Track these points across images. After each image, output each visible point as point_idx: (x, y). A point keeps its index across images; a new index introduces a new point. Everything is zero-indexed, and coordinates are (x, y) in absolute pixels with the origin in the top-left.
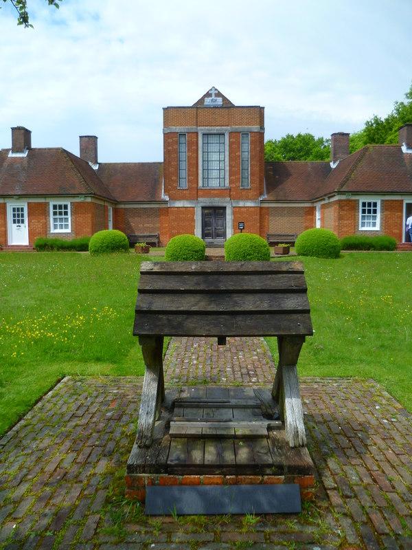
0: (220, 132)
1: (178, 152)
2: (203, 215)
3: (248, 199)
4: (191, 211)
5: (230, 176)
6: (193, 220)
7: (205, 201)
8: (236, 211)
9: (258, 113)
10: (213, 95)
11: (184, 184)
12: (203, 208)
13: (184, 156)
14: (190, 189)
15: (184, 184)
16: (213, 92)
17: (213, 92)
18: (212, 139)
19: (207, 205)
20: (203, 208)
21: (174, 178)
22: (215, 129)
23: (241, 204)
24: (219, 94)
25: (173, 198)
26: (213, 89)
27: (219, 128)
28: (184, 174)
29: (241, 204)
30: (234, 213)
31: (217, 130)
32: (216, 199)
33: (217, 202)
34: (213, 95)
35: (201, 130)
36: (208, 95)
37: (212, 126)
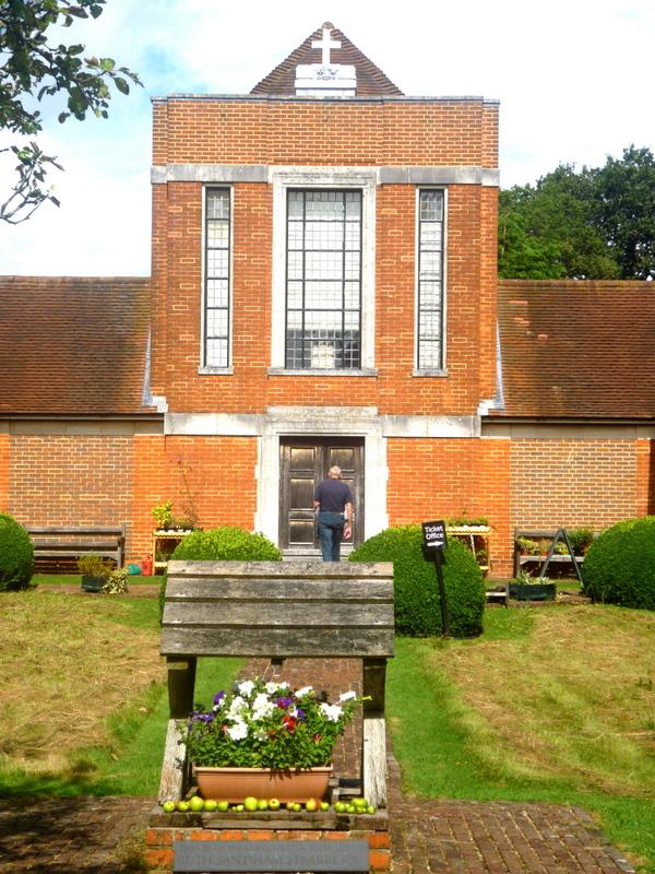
0: (345, 184)
1: (195, 248)
2: (289, 469)
3: (438, 410)
4: (244, 451)
5: (381, 331)
6: (250, 482)
7: (297, 419)
8: (402, 453)
9: (472, 121)
10: (326, 56)
11: (217, 356)
12: (285, 440)
13: (218, 263)
14: (242, 373)
15: (217, 356)
16: (327, 44)
17: (327, 44)
18: (316, 210)
19: (300, 429)
20: (285, 440)
21: (185, 337)
22: (328, 176)
23: (418, 427)
24: (347, 53)
25: (183, 407)
26: (327, 33)
27: (343, 169)
28: (218, 323)
29: (418, 427)
30: (393, 460)
31: (337, 176)
32: (330, 410)
33: (335, 421)
34: (326, 56)
35: (280, 177)
36: (306, 54)
37: (318, 162)
